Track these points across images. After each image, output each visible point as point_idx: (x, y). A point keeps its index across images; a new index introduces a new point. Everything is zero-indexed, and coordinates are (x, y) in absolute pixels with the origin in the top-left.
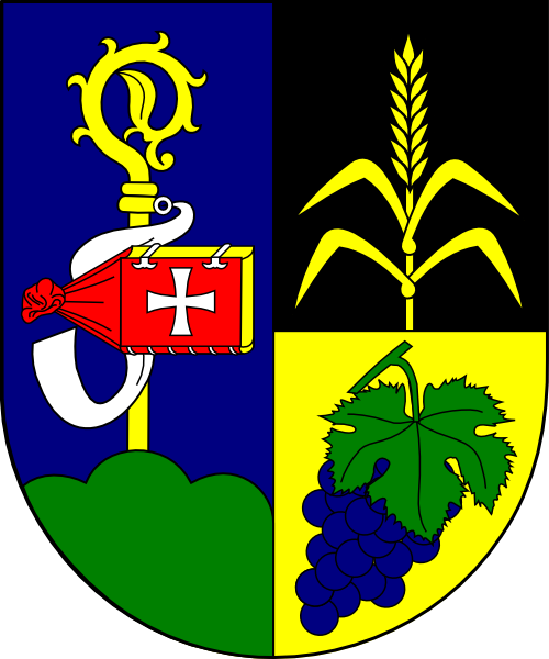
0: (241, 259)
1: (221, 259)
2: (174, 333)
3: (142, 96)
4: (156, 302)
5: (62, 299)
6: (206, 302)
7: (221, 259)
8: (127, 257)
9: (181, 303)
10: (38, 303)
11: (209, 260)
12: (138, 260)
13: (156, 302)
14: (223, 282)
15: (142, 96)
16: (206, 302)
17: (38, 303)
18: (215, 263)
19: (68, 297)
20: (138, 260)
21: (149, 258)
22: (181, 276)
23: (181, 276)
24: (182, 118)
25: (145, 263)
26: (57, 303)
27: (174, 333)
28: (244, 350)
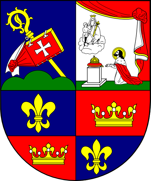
0: (51, 32)
1: (46, 34)
2: (45, 56)
3: (17, 20)
4: (37, 52)
5: (17, 63)
6: (48, 45)
7: (46, 34)
8: (26, 46)
9: (43, 49)
10: (12, 66)
11: (44, 36)
12: (29, 45)
13: (37, 52)
14: (50, 39)
15: (17, 20)
16: (48, 45)
17: (12, 66)
18: (46, 36)
19: (18, 61)
20: (29, 45)
21: (31, 43)
22: (40, 43)
23: (40, 43)
24: (28, 19)
25: (30, 45)
26: (16, 64)
27: (45, 56)
28: (62, 51)
